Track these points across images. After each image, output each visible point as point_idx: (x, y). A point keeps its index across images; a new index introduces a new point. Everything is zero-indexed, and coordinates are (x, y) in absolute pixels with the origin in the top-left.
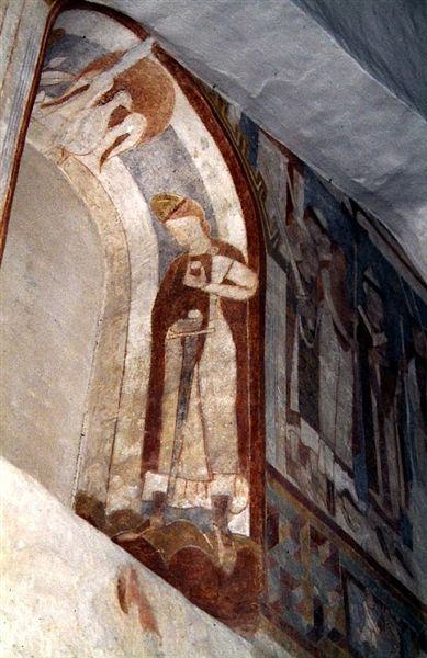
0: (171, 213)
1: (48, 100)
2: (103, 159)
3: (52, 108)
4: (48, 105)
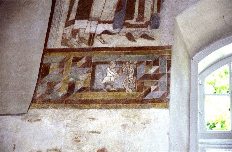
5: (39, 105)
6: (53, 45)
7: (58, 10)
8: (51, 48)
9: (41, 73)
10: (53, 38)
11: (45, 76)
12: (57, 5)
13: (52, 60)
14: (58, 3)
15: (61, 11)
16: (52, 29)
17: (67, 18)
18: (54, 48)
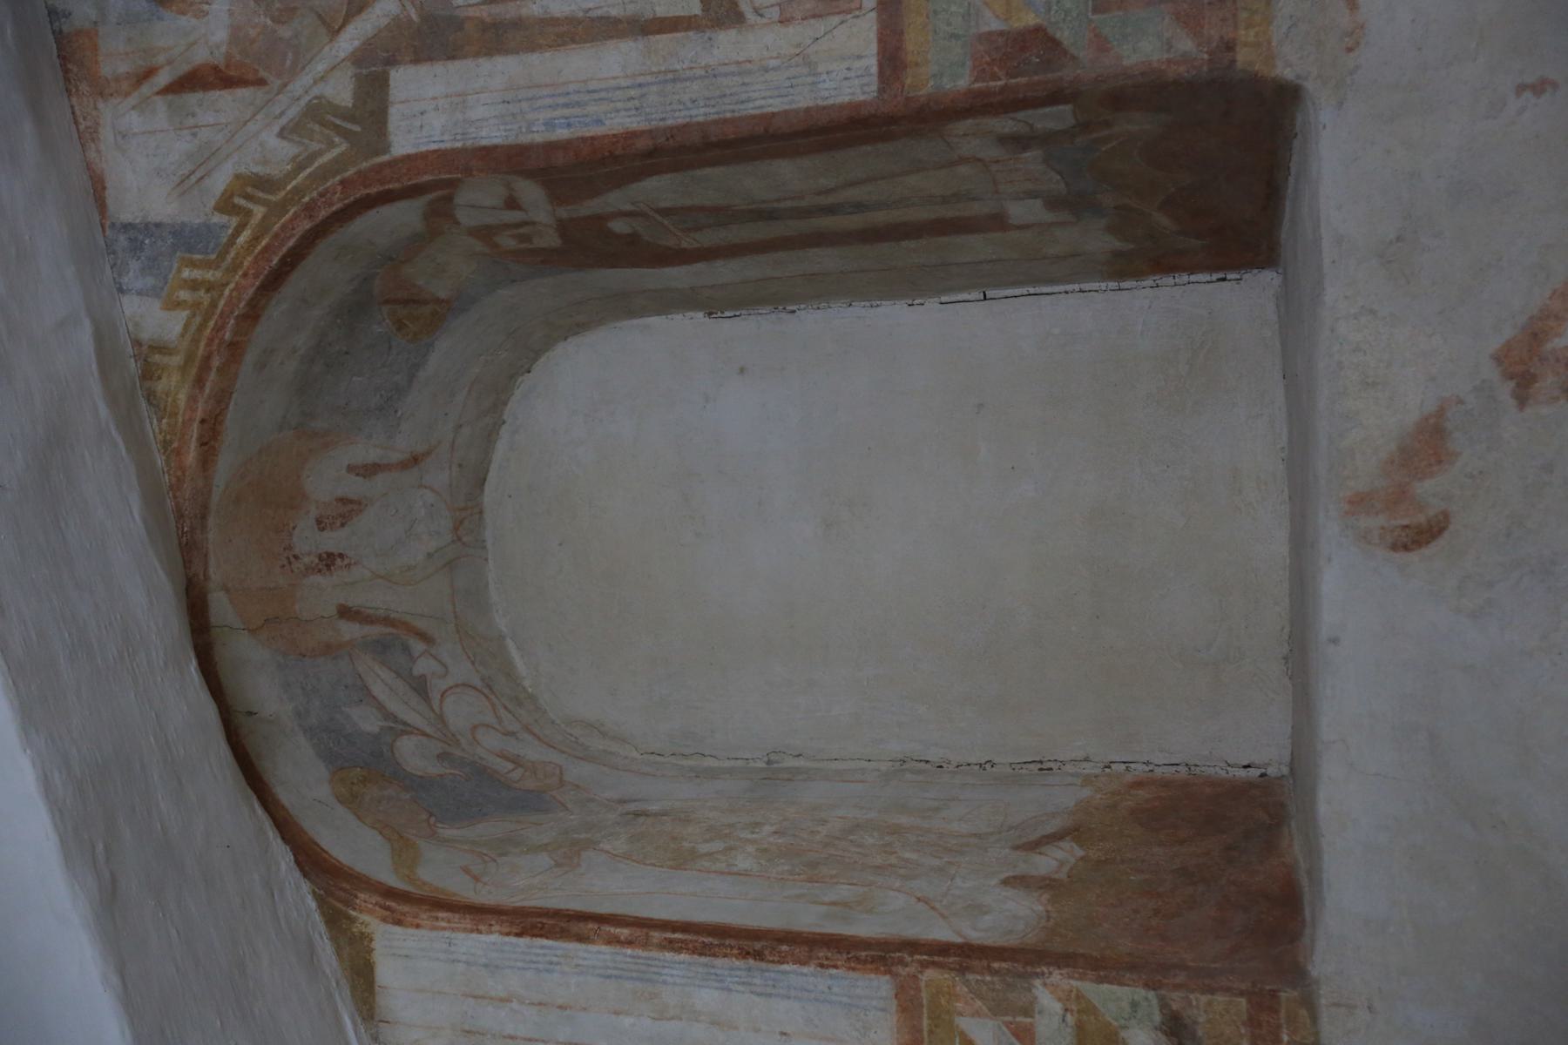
0: (425, 302)
1: (418, 646)
2: (415, 460)
3: (420, 624)
4: (424, 636)
5: (1244, 15)
6: (858, 64)
7: (630, 104)
8: (874, 70)
9: (1036, 78)
10: (810, 79)
11: (1055, 43)
12: (599, 122)
13: (954, 36)
14: (588, 120)
15: (640, 85)
16: (751, 105)
17: (687, 29)
18: (874, 48)
